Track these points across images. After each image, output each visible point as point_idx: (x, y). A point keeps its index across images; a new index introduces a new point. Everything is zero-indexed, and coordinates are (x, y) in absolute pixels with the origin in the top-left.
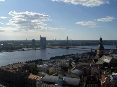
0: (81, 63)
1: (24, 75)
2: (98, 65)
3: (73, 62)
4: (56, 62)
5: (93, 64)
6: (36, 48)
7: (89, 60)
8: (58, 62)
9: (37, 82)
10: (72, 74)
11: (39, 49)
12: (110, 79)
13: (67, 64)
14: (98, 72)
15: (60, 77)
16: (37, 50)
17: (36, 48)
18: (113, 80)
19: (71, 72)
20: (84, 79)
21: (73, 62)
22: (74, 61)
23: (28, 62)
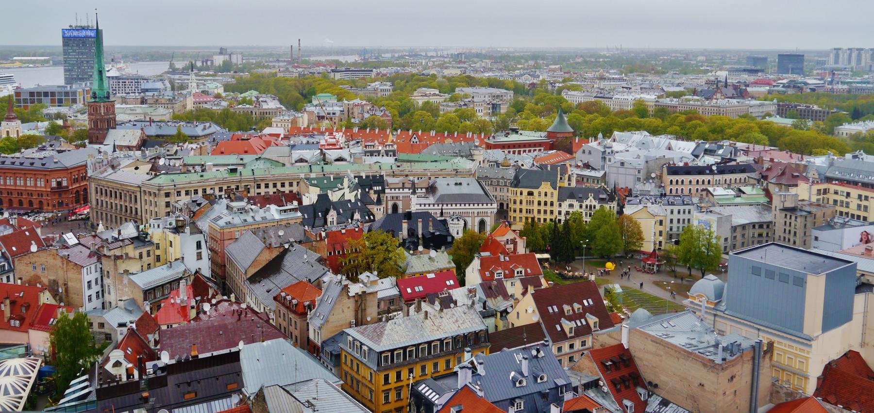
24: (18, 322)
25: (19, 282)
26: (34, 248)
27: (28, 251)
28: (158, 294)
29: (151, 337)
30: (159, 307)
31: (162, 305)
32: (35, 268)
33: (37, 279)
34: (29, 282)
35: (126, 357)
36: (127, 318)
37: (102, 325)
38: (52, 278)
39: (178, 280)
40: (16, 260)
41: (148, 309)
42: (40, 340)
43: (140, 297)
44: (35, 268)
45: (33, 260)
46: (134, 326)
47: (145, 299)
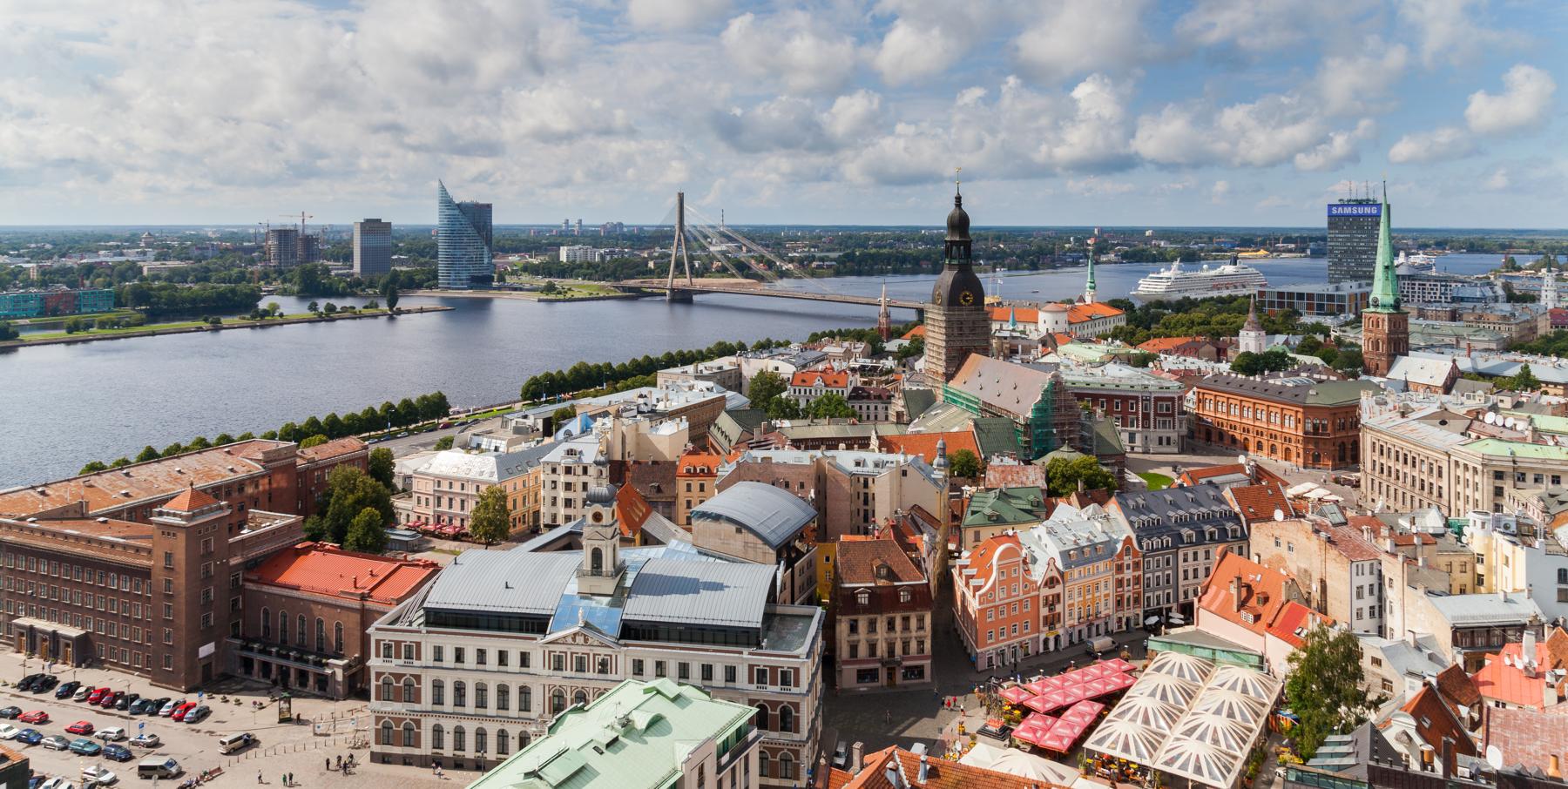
0: (797, 422)
1: (251, 566)
2: (932, 437)
3: (724, 421)
4: (574, 426)
5: (889, 430)
6: (392, 304)
7: (857, 394)
8: (594, 418)
9: (376, 624)
10: (708, 523)
11: (421, 311)
12: (1035, 561)
13: (669, 437)
14: (935, 503)
15: (597, 555)
16: (400, 312)
17: (392, 304)
18: (1060, 565)
19: (710, 505)
20: (810, 563)
21: (724, 421)
22: (729, 412)
23: (296, 434)
24: (1251, 617)
25: (1256, 559)
26: (1279, 515)
27: (1270, 518)
28: (1480, 641)
29: (1464, 711)
30: (1480, 665)
31: (1487, 662)
32: (1277, 544)
33: (1281, 559)
34: (1270, 563)
35: (1419, 729)
36: (1420, 663)
37: (1377, 662)
38: (1303, 566)
39: (1521, 628)
40: (1253, 526)
41: (1460, 660)
42: (1279, 653)
43: (1445, 638)
44: (1277, 544)
45: (1277, 533)
46: (1434, 682)
47: (1455, 643)
